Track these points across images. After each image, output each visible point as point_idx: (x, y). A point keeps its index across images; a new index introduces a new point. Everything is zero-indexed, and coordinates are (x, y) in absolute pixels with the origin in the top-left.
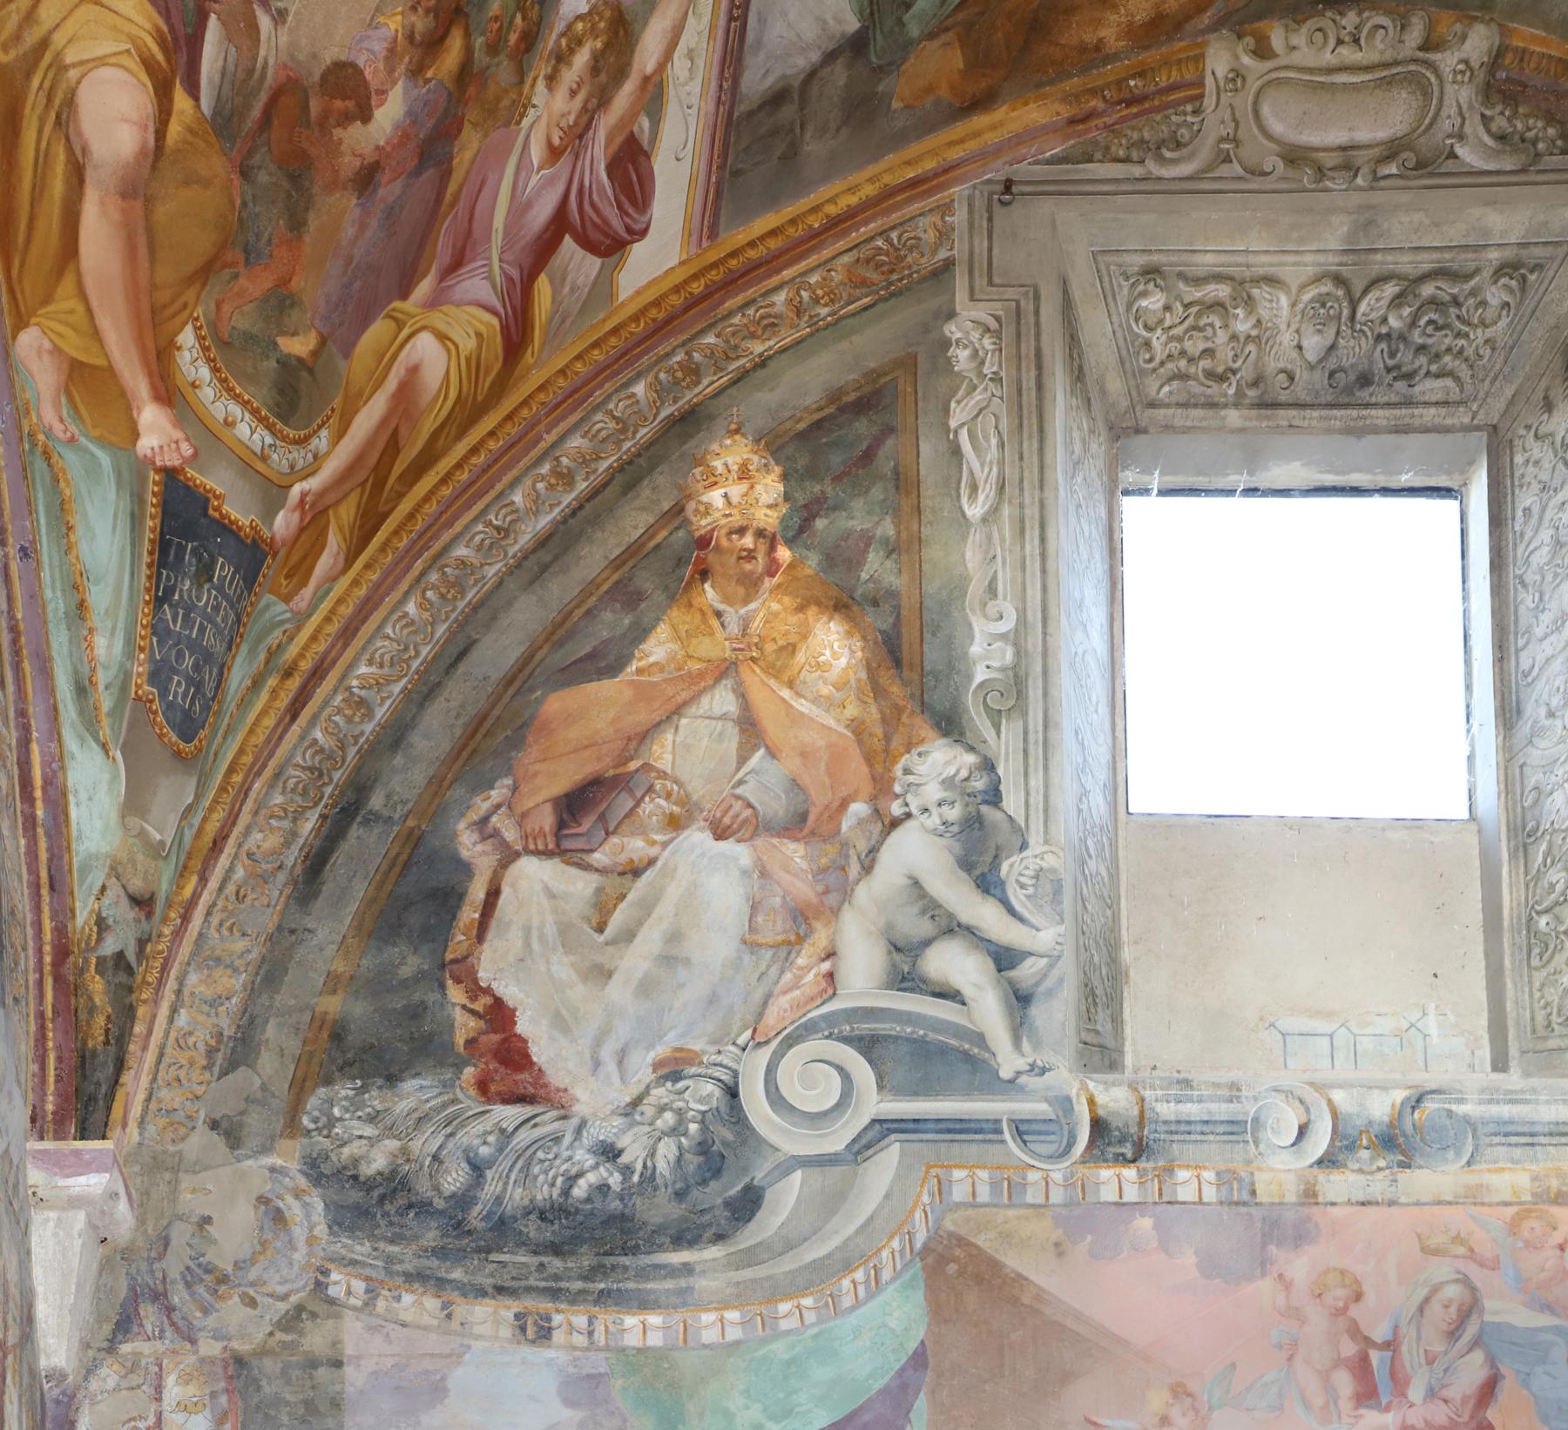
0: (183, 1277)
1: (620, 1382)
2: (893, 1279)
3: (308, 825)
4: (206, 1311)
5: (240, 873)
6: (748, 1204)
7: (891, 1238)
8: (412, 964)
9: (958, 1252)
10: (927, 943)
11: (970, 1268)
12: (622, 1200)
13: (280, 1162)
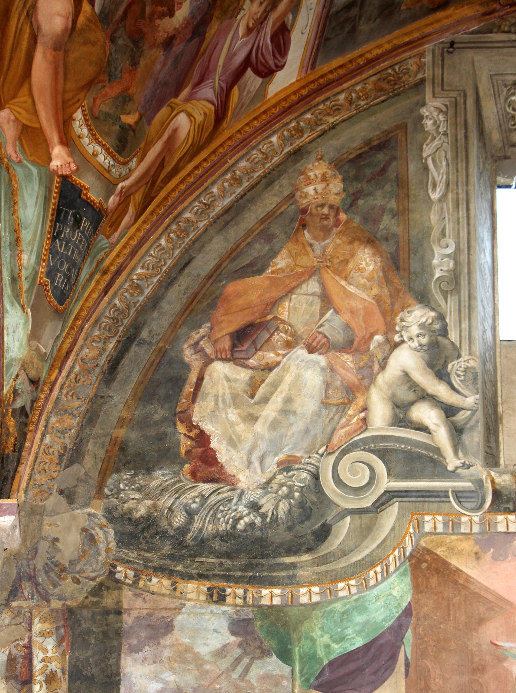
0: (44, 568)
1: (259, 623)
2: (395, 571)
3: (111, 346)
4: (55, 586)
5: (77, 368)
6: (324, 533)
7: (394, 550)
8: (160, 413)
9: (427, 557)
11: (433, 565)
12: (261, 530)
13: (93, 511)
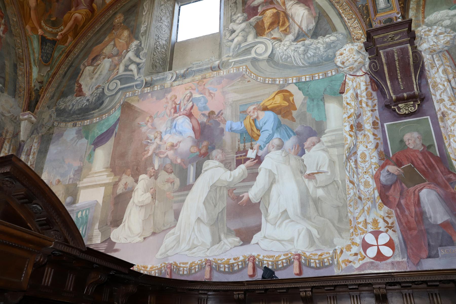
10: (129, 65)
